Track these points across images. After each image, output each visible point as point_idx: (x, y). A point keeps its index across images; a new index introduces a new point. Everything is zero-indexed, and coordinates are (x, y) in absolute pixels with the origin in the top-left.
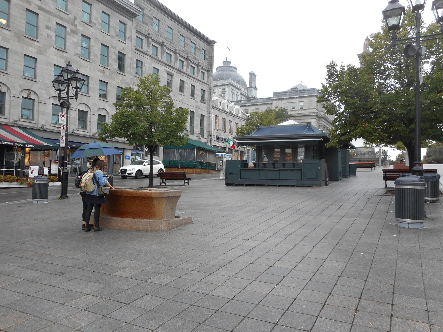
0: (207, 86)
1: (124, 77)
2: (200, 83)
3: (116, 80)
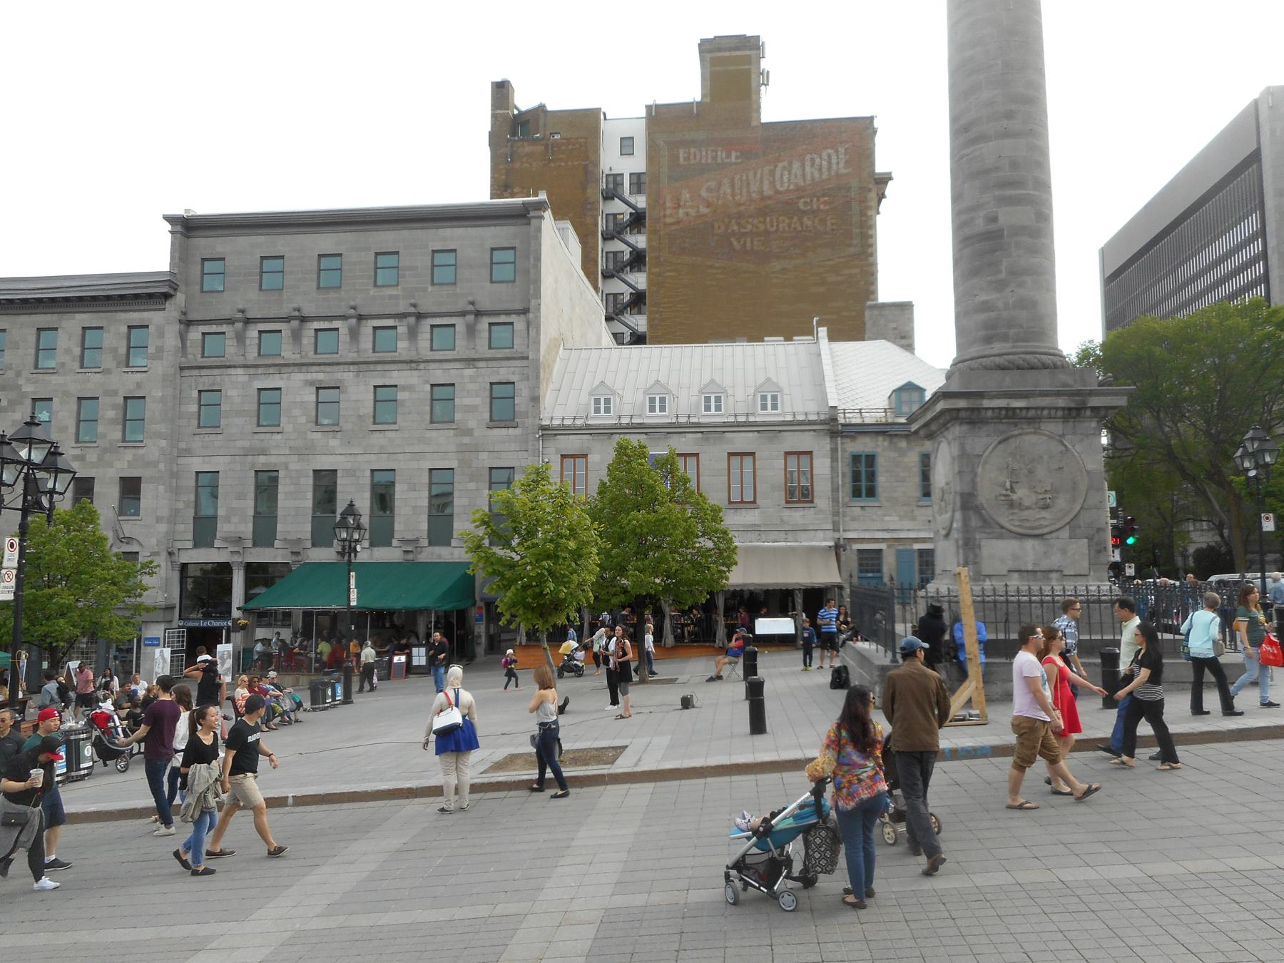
0: (524, 363)
1: (141, 451)
2: (481, 364)
3: (118, 465)
